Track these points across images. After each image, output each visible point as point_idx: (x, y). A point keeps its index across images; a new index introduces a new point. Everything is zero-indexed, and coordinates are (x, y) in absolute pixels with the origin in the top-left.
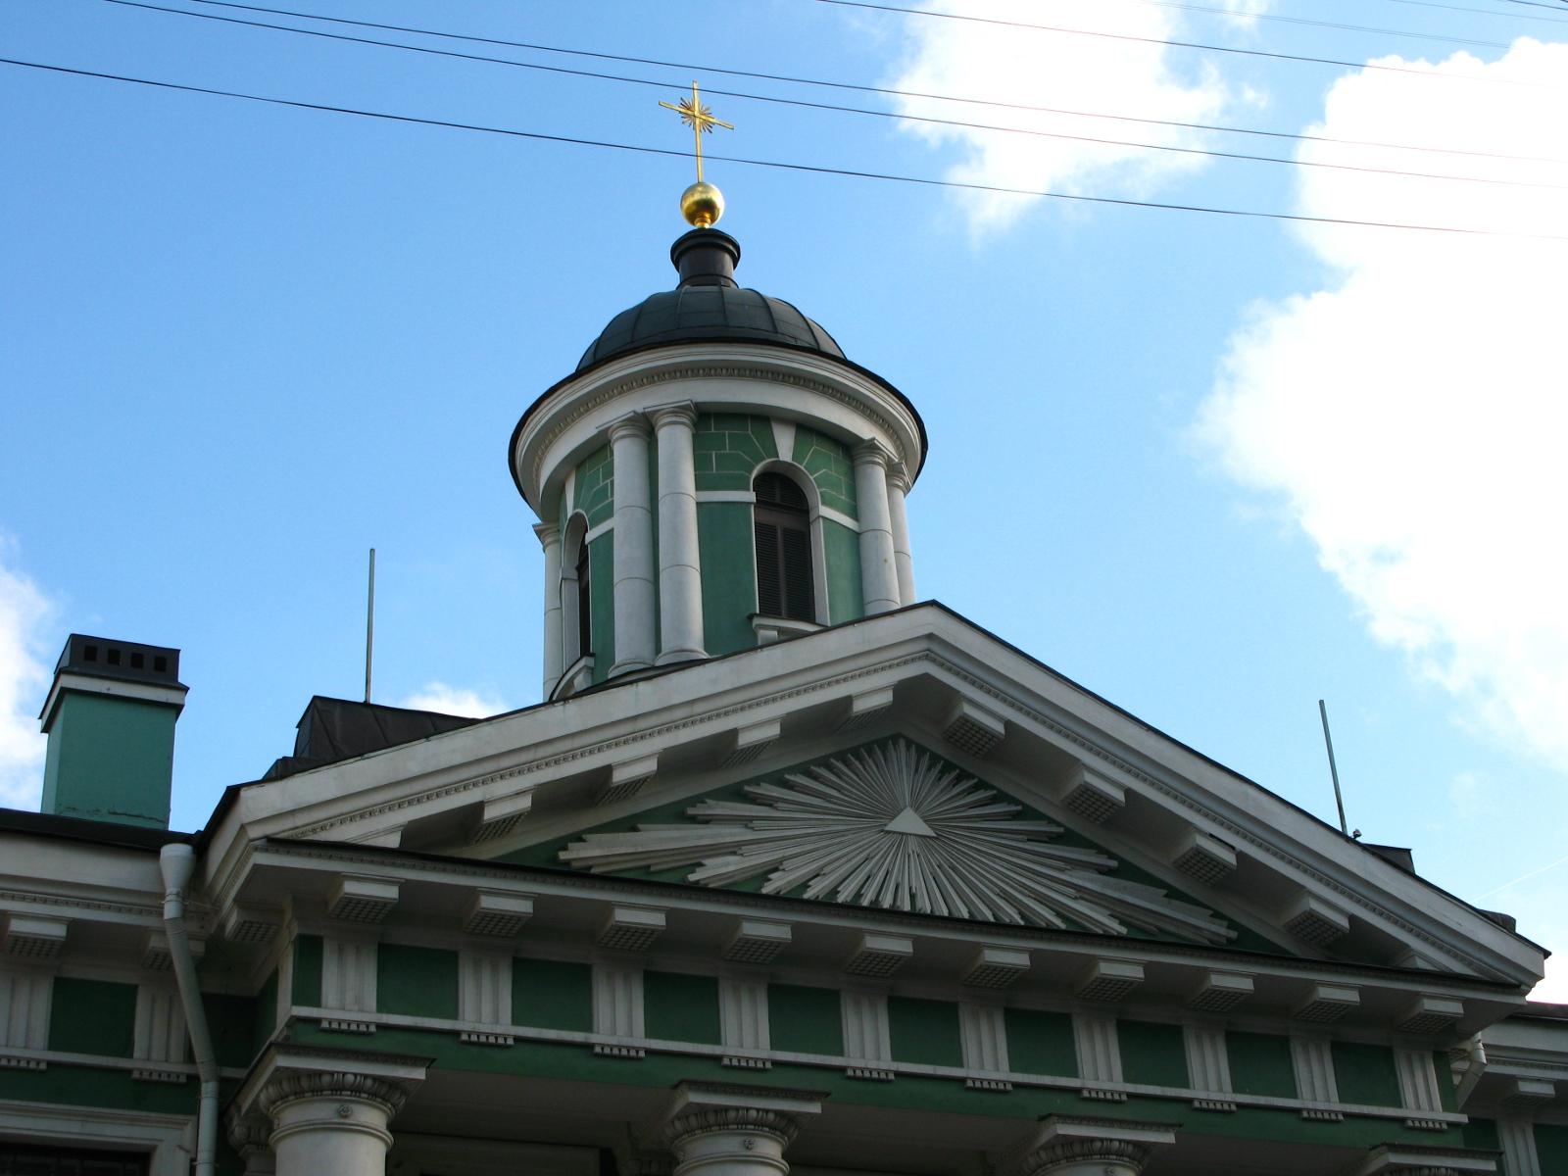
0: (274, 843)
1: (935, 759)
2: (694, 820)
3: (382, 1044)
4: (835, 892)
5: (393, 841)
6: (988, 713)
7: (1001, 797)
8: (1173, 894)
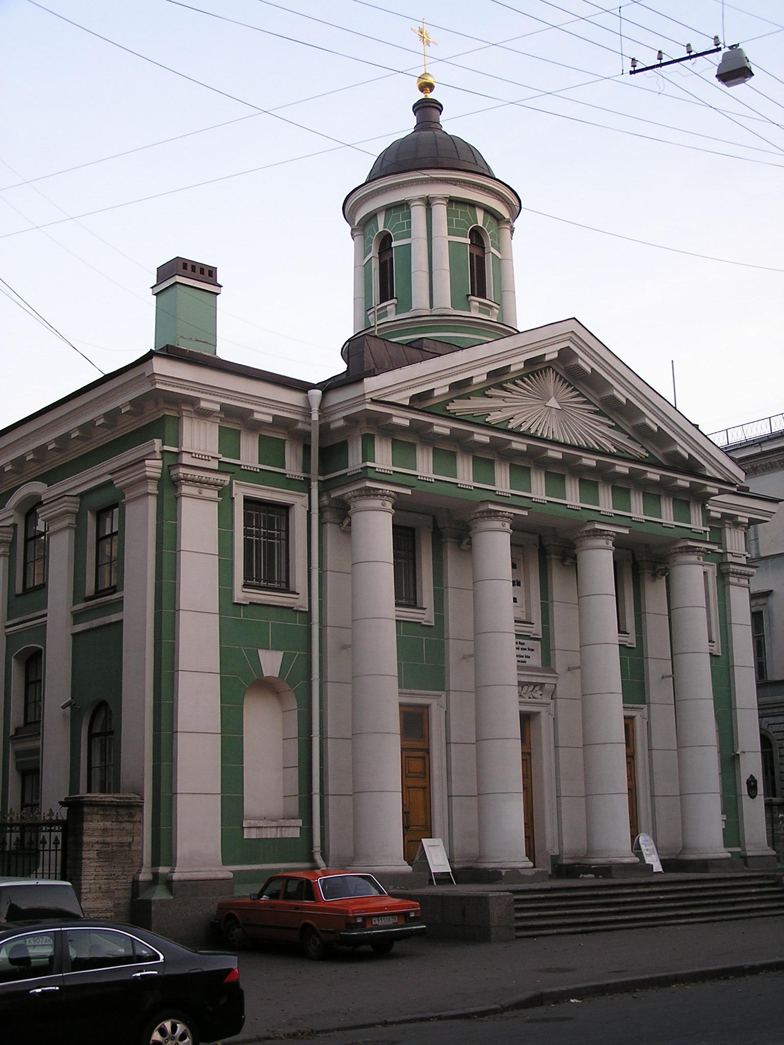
0: (374, 401)
3: (394, 479)
4: (508, 421)
5: (407, 403)
6: (586, 363)
7: (580, 395)
8: (630, 438)
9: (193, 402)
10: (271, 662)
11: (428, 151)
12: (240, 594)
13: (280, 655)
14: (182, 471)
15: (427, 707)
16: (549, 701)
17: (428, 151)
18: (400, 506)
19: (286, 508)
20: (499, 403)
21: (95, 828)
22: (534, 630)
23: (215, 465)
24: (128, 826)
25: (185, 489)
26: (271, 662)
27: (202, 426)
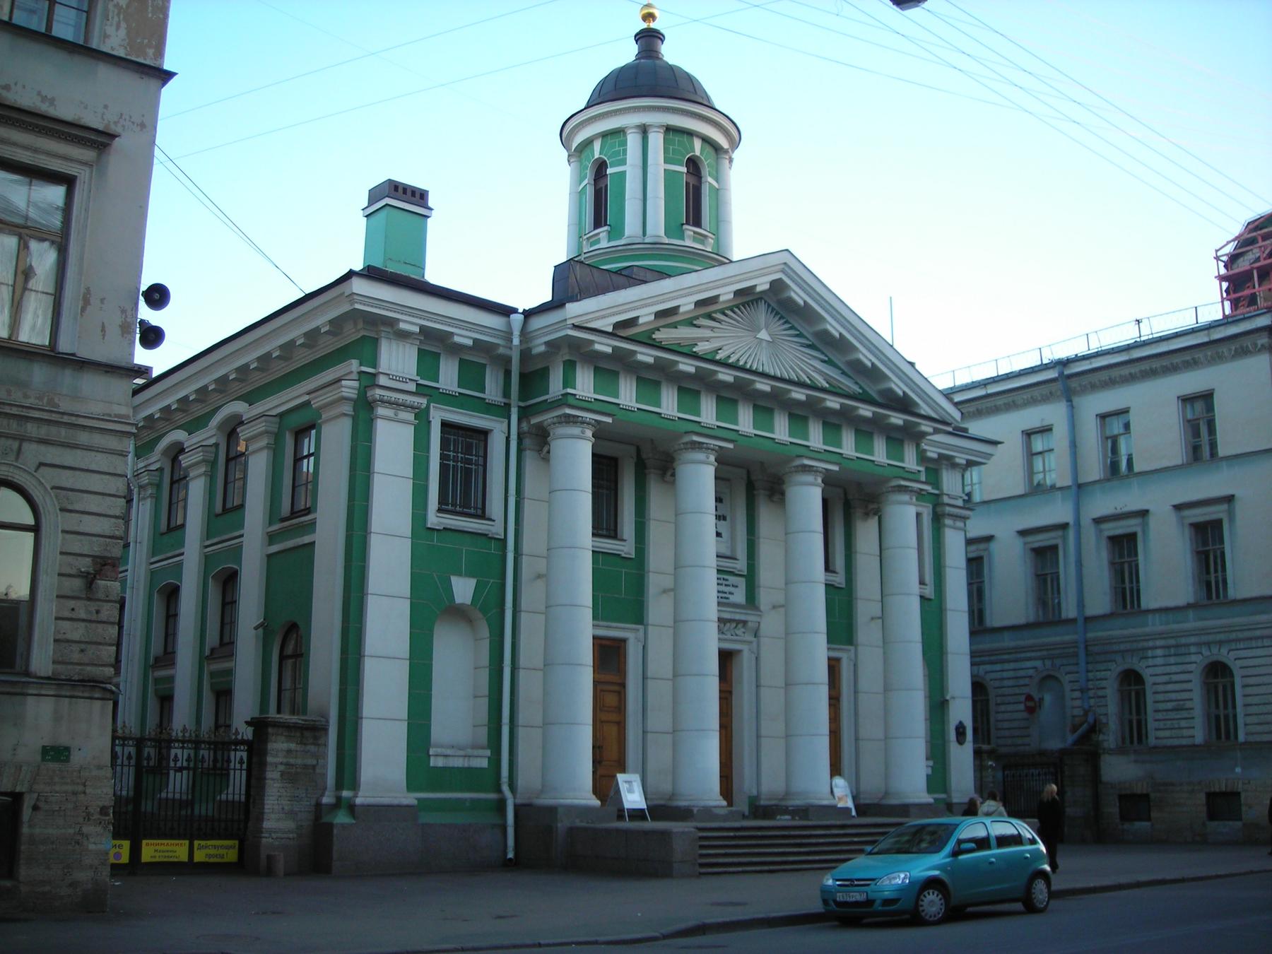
0: (575, 327)
1: (773, 309)
2: (695, 326)
4: (716, 351)
5: (610, 329)
6: (798, 296)
7: (792, 328)
8: (844, 373)
9: (391, 322)
10: (463, 589)
11: (648, 78)
12: (433, 519)
13: (472, 583)
14: (378, 392)
15: (624, 641)
16: (751, 638)
17: (648, 78)
18: (601, 434)
19: (484, 434)
20: (707, 333)
21: (279, 748)
22: (738, 566)
23: (412, 387)
24: (312, 748)
25: (381, 411)
26: (463, 589)
27: (401, 348)
